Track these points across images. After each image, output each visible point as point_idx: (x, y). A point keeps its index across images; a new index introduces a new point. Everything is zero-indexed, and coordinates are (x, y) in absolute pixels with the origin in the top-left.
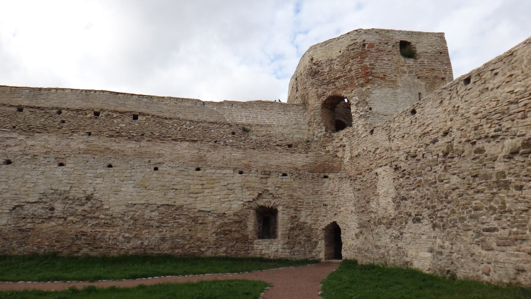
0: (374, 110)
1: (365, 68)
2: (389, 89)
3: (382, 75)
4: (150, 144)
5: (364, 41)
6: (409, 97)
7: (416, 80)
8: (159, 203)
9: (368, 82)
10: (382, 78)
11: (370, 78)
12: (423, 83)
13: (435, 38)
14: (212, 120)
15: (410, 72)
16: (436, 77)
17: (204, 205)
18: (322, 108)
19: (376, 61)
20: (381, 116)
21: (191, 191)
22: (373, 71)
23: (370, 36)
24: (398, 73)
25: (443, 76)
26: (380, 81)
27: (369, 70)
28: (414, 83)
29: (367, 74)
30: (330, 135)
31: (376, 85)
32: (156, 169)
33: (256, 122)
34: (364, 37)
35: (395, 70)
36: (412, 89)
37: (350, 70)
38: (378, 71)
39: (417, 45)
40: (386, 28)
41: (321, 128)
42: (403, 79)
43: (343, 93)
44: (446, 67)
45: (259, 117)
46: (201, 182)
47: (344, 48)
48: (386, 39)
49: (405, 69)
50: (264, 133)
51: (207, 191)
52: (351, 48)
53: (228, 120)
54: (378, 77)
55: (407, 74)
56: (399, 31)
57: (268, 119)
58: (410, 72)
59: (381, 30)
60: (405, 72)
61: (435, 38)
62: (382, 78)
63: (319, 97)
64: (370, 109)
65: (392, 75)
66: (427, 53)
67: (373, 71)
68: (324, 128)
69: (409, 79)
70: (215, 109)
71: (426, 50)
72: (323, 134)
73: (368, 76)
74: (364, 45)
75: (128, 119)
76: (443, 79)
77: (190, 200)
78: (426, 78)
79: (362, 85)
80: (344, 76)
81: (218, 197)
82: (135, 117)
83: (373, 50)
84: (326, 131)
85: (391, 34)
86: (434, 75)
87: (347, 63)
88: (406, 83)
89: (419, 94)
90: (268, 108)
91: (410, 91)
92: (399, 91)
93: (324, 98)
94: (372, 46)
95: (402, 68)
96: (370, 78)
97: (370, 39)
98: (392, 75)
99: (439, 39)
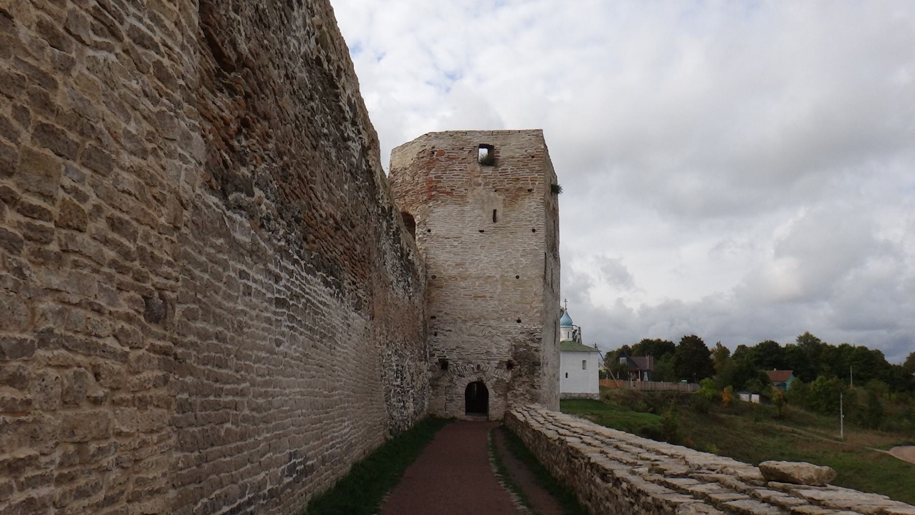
0: (433, 232)
1: (431, 181)
2: (455, 206)
3: (448, 190)
6: (479, 216)
7: (492, 194)
9: (431, 198)
10: (448, 193)
11: (433, 193)
12: (501, 197)
13: (528, 137)
15: (486, 184)
19: (444, 172)
22: (439, 185)
23: (441, 141)
24: (470, 185)
25: (531, 187)
26: (444, 197)
28: (489, 198)
34: (434, 143)
35: (466, 182)
36: (486, 206)
37: (417, 184)
38: (445, 184)
39: (502, 148)
40: (464, 129)
42: (475, 192)
47: (415, 156)
48: (461, 143)
49: (480, 180)
52: (421, 156)
54: (443, 192)
55: (482, 187)
56: (480, 132)
58: (486, 184)
59: (457, 132)
60: (480, 185)
61: (528, 137)
62: (448, 193)
64: (429, 231)
65: (462, 189)
66: (513, 158)
67: (439, 185)
69: (483, 193)
71: (513, 154)
73: (434, 192)
74: (433, 153)
76: (530, 191)
78: (507, 190)
79: (426, 202)
83: (442, 158)
85: (469, 137)
86: (517, 186)
87: (416, 174)
88: (479, 198)
89: (495, 211)
91: (482, 208)
92: (468, 208)
94: (441, 153)
95: (476, 179)
96: (433, 193)
97: (441, 145)
98: (462, 189)
99: (533, 138)
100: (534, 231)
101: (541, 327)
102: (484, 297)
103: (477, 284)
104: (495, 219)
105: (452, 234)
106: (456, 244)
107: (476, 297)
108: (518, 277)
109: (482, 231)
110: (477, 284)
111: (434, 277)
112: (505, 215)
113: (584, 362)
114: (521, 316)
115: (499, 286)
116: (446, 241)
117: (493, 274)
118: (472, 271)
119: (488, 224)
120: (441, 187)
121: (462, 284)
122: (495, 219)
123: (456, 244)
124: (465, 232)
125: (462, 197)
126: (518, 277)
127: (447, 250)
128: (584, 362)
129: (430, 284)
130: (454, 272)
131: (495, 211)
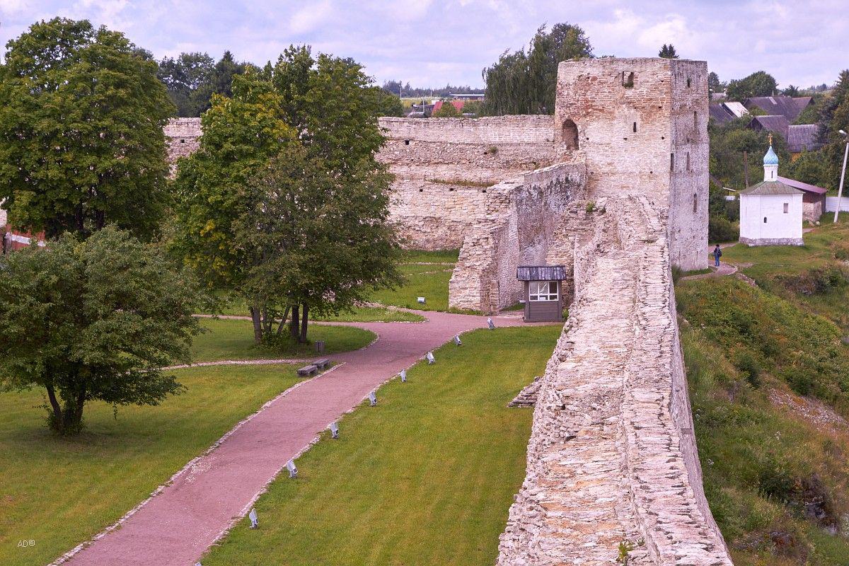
0: (590, 140)
3: (601, 108)
4: (418, 168)
5: (588, 74)
8: (424, 216)
10: (600, 110)
11: (590, 110)
12: (639, 114)
14: (469, 141)
16: (653, 107)
17: (456, 217)
18: (564, 128)
20: (596, 145)
21: (447, 206)
22: (593, 104)
23: (595, 69)
27: (590, 103)
29: (587, 107)
30: (570, 153)
31: (594, 117)
32: (421, 191)
33: (508, 141)
38: (598, 103)
41: (563, 146)
43: (574, 119)
44: (664, 96)
45: (512, 134)
46: (453, 200)
48: (610, 70)
50: (512, 152)
51: (457, 206)
53: (483, 139)
57: (519, 136)
62: (600, 110)
63: (561, 118)
64: (588, 139)
65: (611, 107)
67: (593, 104)
68: (565, 146)
70: (472, 130)
72: (563, 152)
74: (589, 78)
75: (402, 145)
76: (660, 107)
77: (447, 213)
78: (643, 108)
79: (585, 116)
80: (575, 104)
81: (467, 211)
82: (407, 143)
84: (568, 148)
85: (615, 66)
89: (635, 124)
90: (520, 125)
92: (615, 122)
93: (564, 120)
94: (594, 79)
96: (590, 110)
100: (663, 138)
101: (667, 208)
102: (628, 187)
103: (623, 177)
104: (635, 130)
105: (604, 141)
106: (607, 148)
107: (622, 187)
108: (651, 172)
109: (626, 139)
110: (623, 177)
111: (592, 173)
112: (642, 126)
113: (786, 205)
114: (654, 200)
115: (639, 179)
116: (600, 146)
117: (634, 170)
118: (620, 168)
119: (630, 134)
120: (594, 106)
121: (612, 178)
122: (635, 130)
123: (607, 148)
124: (613, 139)
125: (611, 113)
126: (651, 172)
127: (601, 153)
128: (786, 205)
129: (590, 178)
130: (606, 169)
131: (635, 124)
